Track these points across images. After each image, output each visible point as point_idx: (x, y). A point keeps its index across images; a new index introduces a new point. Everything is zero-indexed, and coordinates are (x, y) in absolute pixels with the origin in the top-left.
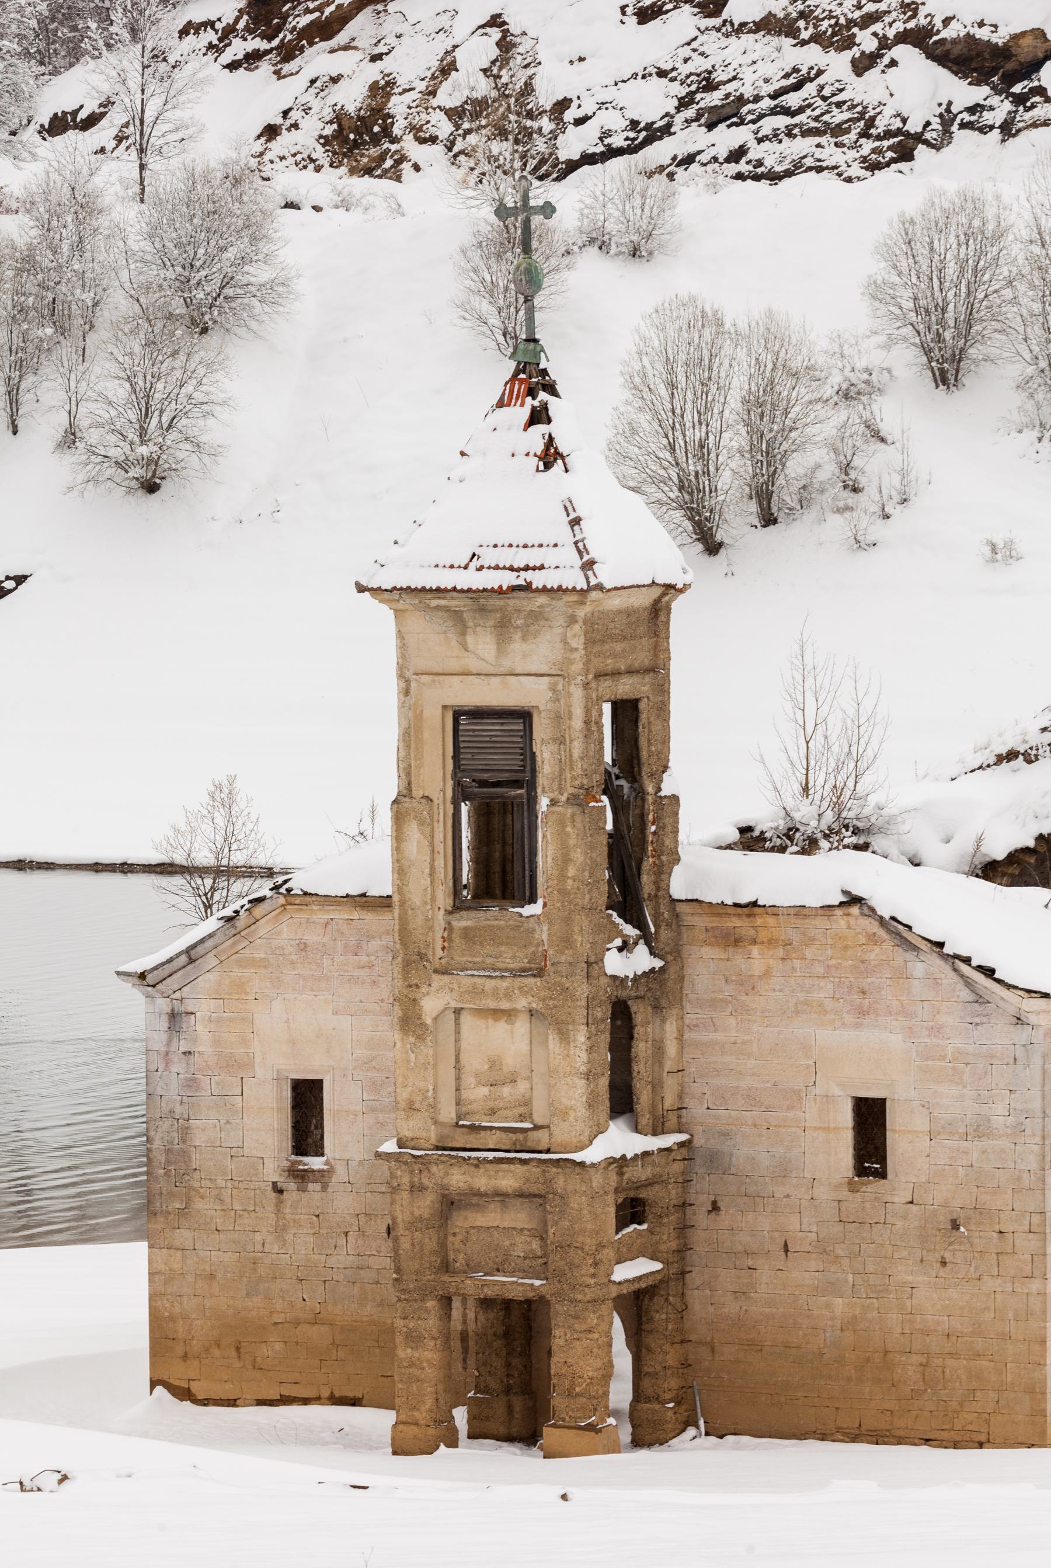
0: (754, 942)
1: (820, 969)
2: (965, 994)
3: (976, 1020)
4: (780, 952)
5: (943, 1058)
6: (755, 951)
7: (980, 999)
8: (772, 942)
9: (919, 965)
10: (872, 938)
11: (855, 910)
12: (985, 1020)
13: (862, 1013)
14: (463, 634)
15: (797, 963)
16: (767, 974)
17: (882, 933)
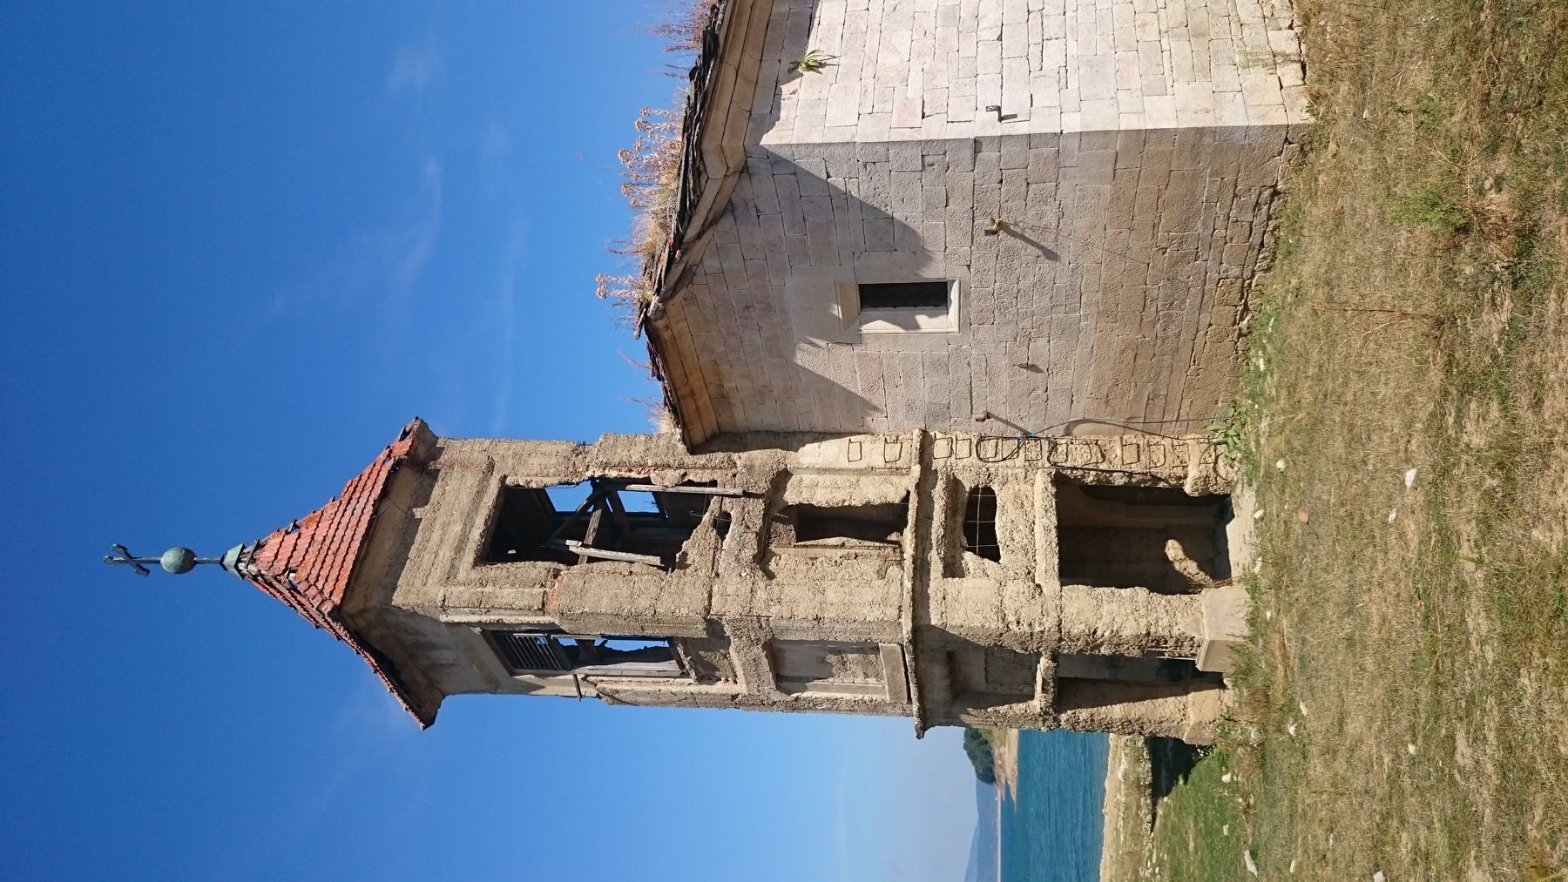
0: (721, 386)
1: (733, 341)
2: (726, 223)
3: (753, 212)
4: (725, 368)
5: (802, 241)
6: (727, 385)
7: (729, 209)
8: (718, 374)
9: (707, 262)
10: (692, 300)
11: (660, 324)
12: (751, 204)
13: (769, 308)
14: (442, 666)
15: (732, 356)
16: (749, 377)
17: (679, 297)
